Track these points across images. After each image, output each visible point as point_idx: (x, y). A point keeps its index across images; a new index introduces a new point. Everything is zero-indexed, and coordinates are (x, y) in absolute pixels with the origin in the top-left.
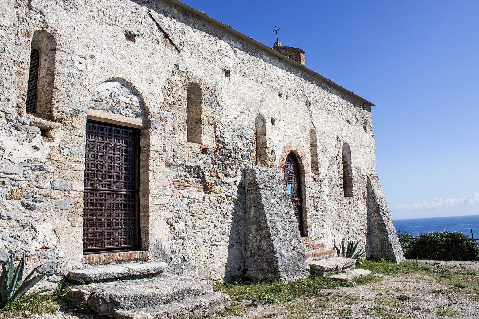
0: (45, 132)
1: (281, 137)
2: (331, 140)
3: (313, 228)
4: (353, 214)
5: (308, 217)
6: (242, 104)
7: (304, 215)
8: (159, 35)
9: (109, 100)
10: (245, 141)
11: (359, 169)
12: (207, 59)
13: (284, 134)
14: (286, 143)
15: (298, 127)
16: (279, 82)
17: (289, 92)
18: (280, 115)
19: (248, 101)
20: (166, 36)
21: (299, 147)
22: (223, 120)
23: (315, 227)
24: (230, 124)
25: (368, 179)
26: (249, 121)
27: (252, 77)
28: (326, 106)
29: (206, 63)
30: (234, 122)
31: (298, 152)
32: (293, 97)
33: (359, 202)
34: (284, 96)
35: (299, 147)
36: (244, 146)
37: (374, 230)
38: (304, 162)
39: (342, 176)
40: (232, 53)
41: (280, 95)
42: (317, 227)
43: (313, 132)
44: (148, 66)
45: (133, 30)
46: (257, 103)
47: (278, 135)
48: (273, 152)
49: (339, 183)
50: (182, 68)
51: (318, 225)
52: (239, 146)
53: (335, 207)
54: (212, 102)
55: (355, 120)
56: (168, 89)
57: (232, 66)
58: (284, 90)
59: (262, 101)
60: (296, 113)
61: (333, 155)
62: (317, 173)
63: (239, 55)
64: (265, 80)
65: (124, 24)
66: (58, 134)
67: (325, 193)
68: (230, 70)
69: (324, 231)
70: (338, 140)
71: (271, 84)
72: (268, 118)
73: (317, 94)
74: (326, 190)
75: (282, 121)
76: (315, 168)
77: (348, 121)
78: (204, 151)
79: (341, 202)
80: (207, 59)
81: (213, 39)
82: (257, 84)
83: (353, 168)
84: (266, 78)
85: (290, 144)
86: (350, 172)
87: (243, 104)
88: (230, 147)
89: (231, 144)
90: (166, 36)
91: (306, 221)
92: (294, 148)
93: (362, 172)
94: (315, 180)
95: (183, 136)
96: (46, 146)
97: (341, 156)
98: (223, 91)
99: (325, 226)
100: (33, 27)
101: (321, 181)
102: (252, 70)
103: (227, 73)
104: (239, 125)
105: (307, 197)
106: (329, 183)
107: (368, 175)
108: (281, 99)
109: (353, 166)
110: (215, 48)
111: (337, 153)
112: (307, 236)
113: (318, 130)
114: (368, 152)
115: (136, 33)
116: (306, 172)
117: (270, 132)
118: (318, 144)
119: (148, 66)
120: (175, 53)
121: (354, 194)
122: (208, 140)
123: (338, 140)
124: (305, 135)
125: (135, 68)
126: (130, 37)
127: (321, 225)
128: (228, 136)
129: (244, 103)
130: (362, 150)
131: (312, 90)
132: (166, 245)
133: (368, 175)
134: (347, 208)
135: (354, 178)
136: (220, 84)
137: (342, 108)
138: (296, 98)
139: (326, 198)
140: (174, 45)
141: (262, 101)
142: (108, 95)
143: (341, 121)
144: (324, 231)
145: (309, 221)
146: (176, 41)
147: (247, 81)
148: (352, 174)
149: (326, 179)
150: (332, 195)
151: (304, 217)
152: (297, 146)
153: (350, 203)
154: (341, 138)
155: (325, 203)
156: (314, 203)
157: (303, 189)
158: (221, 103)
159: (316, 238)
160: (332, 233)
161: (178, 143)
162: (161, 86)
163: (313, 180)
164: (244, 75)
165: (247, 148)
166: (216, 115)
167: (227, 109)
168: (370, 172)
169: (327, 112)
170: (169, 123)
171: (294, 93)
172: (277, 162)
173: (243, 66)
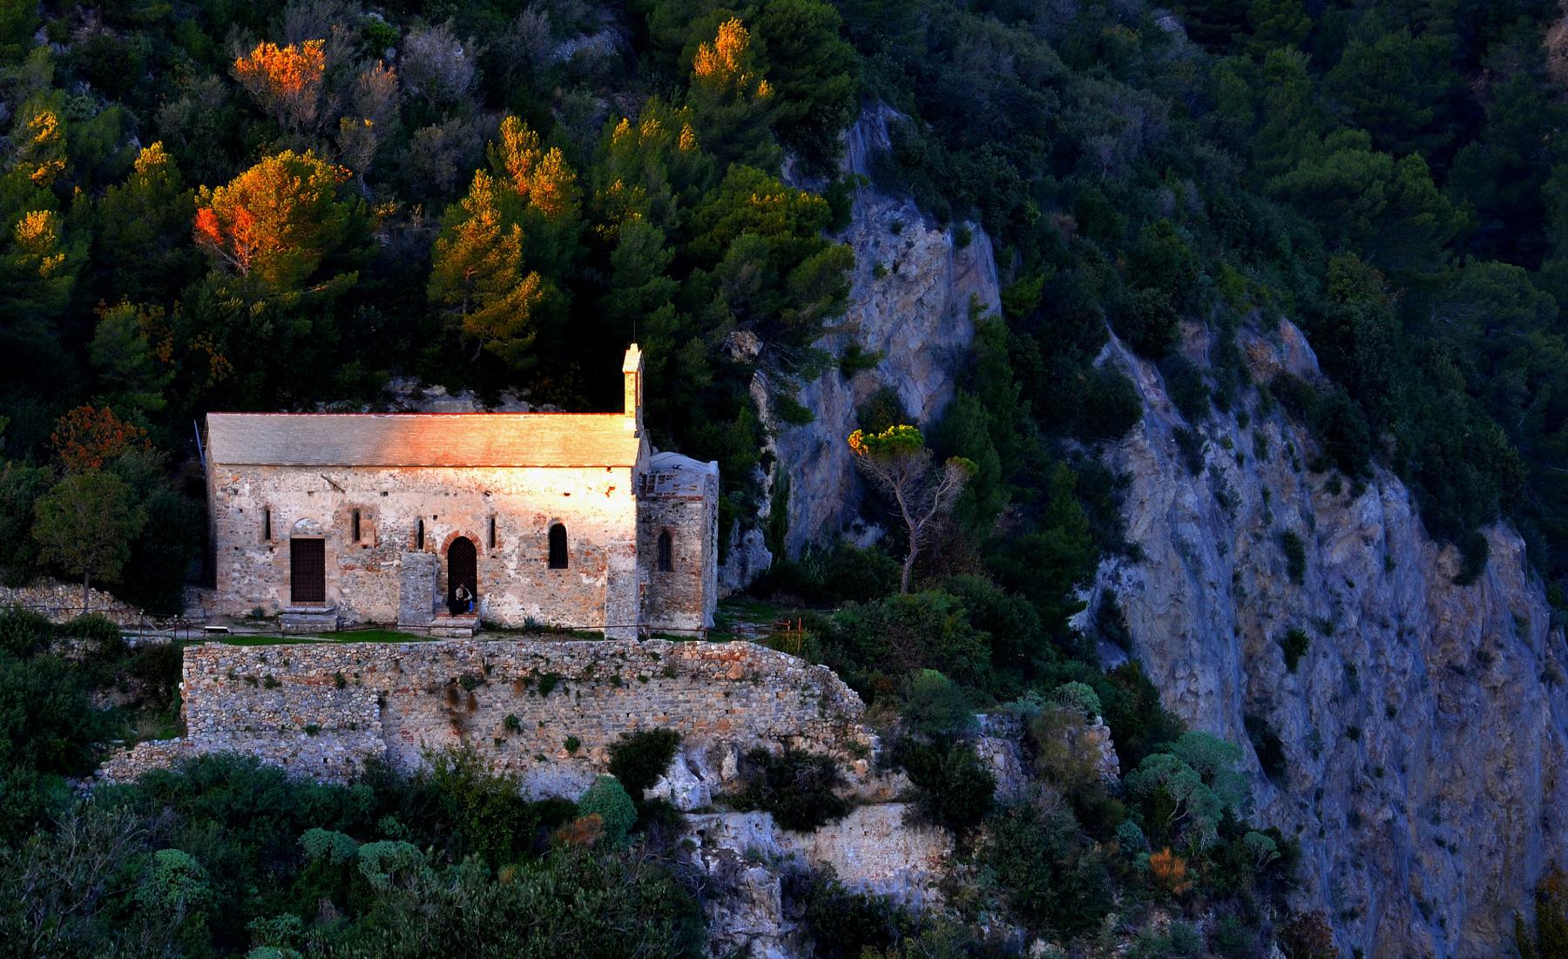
0: (271, 549)
1: (445, 528)
8: (328, 486)
10: (403, 537)
22: (381, 527)
26: (408, 522)
34: (451, 495)
38: (476, 545)
44: (323, 507)
49: (538, 557)
50: (347, 501)
56: (337, 516)
58: (451, 491)
65: (306, 488)
66: (276, 550)
78: (365, 547)
85: (457, 532)
95: (349, 541)
96: (271, 556)
100: (261, 505)
103: (386, 494)
110: (373, 481)
117: (429, 525)
120: (340, 494)
122: (365, 540)
126: (310, 493)
132: (337, 600)
139: (512, 573)
144: (505, 599)
146: (342, 487)
147: (405, 494)
164: (403, 491)
172: (439, 547)
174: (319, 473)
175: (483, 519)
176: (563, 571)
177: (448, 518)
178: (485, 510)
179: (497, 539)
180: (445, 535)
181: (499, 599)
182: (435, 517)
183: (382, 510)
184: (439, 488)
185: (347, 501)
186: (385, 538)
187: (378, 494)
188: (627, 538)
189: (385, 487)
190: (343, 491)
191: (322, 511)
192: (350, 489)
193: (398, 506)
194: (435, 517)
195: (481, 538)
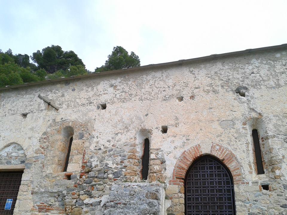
1: (178, 142)
6: (118, 126)
9: (6, 157)
10: (119, 159)
12: (83, 105)
13: (184, 139)
14: (187, 148)
16: (178, 87)
19: (126, 121)
20: (49, 104)
21: (218, 147)
24: (102, 147)
27: (133, 99)
29: (81, 108)
30: (107, 144)
31: (215, 154)
36: (117, 164)
38: (231, 166)
40: (111, 90)
41: (181, 99)
45: (24, 112)
46: (140, 119)
47: (173, 142)
50: (58, 119)
52: (110, 164)
54: (83, 135)
57: (109, 99)
59: (147, 115)
63: (118, 88)
64: (153, 94)
68: (107, 103)
71: (164, 93)
72: (157, 128)
80: (83, 105)
81: (90, 89)
82: (141, 101)
84: (156, 90)
85: (198, 147)
87: (120, 126)
88: (99, 168)
89: (99, 166)
90: (49, 104)
92: (205, 150)
98: (96, 122)
102: (134, 93)
103: (104, 107)
104: (113, 146)
115: (28, 112)
119: (32, 129)
125: (22, 133)
128: (96, 159)
129: (121, 124)
136: (93, 118)
140: (54, 108)
141: (147, 115)
142: (6, 154)
147: (126, 105)
158: (94, 133)
161: (44, 174)
162: (38, 138)
164: (123, 100)
165: (121, 165)
166: (87, 144)
167: (99, 136)
170: (40, 162)
173: (123, 94)
174: (37, 94)
175: (239, 125)
177: (183, 129)
179: (266, 158)
180: (178, 153)
182: (165, 130)
183: (98, 126)
184: (169, 92)
185: (58, 119)
186: (95, 162)
187: (93, 107)
189: (102, 99)
190: (57, 109)
191: (30, 134)
192: (64, 106)
193: (117, 118)
194: (165, 130)
195: (238, 155)
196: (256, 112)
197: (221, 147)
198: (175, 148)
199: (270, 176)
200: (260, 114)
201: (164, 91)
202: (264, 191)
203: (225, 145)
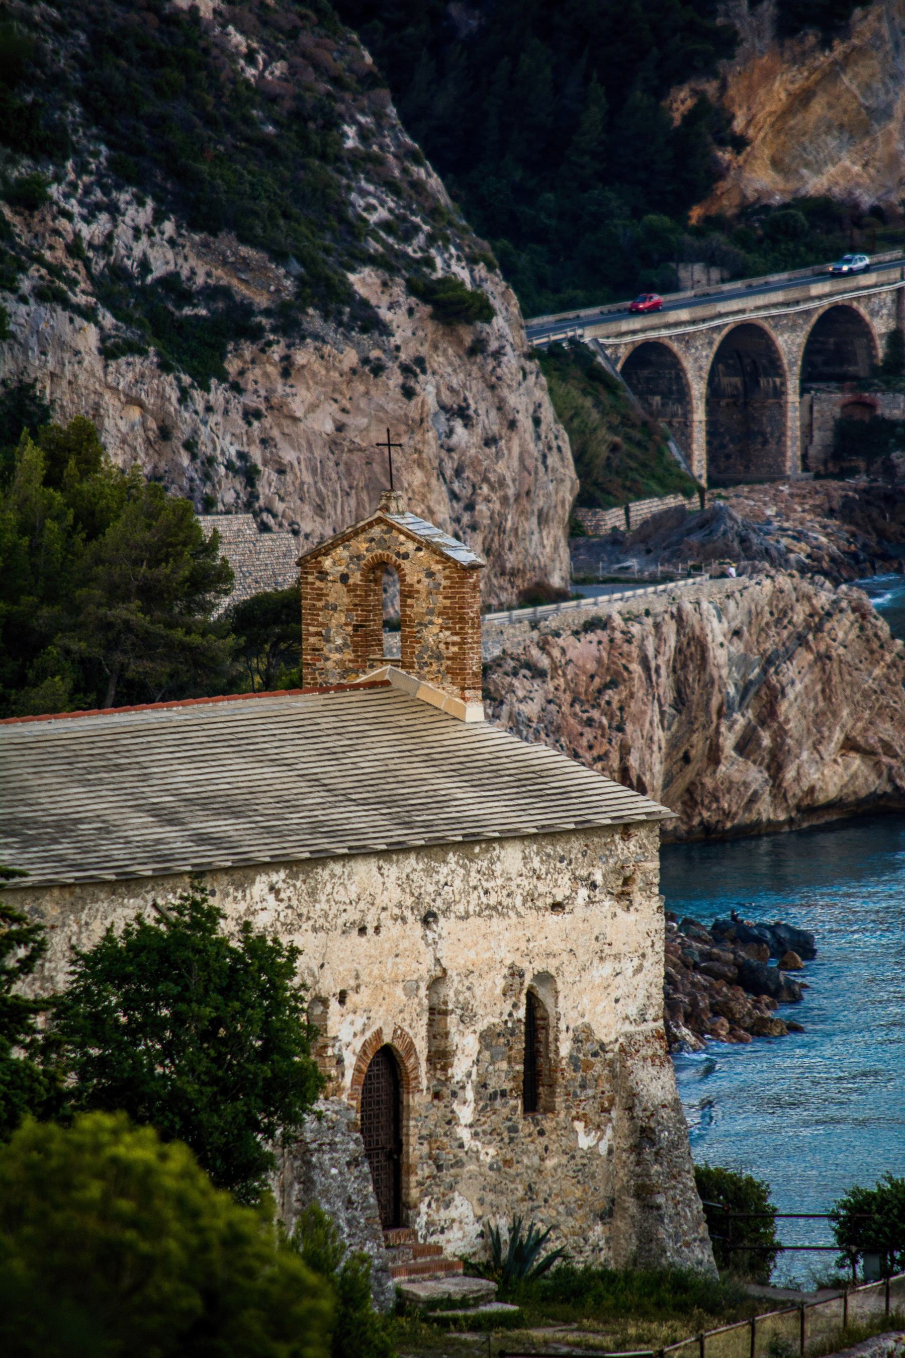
2: (490, 984)
3: (423, 1208)
4: (550, 1163)
5: (413, 1184)
7: (404, 1178)
11: (582, 1036)
14: (368, 1035)
15: (399, 991)
17: (384, 915)
18: (357, 977)
21: (399, 1032)
23: (429, 1206)
25: (622, 1050)
28: (484, 899)
32: (390, 923)
33: (579, 1126)
34: (370, 931)
35: (399, 1032)
37: (625, 1201)
39: (520, 1068)
41: (362, 931)
42: (434, 1205)
43: (437, 982)
47: (352, 1023)
48: (340, 1061)
49: (507, 1086)
51: (437, 1200)
53: (489, 1153)
55: (583, 893)
60: (397, 956)
61: (496, 1021)
62: (443, 1078)
67: (463, 1122)
69: (453, 1213)
70: (516, 973)
73: (458, 883)
74: (466, 1113)
75: (363, 988)
76: (439, 1066)
77: (557, 907)
79: (513, 1135)
83: (562, 1036)
85: (379, 1033)
86: (552, 1047)
91: (408, 1195)
92: (387, 1039)
93: (602, 1034)
94: (437, 1096)
97: (521, 1013)
99: (458, 1199)
101: (454, 1094)
105: (413, 1140)
106: (477, 1093)
107: (621, 1040)
108: (364, 940)
109: (562, 1026)
111: (508, 1008)
112: (408, 1227)
113: (454, 974)
114: (630, 972)
116: (413, 1084)
118: (451, 1007)
121: (559, 1102)
123: (516, 973)
124: (416, 1000)
127: (447, 1198)
130: (607, 968)
131: (442, 882)
133: (621, 1040)
134: (531, 1147)
135: (564, 1062)
137: (539, 878)
138: (399, 921)
139: (464, 1134)
143: (531, 917)
144: (453, 1213)
145: (414, 1193)
148: (557, 1051)
149: (469, 1087)
150: (485, 1123)
151: (404, 1185)
152: (395, 1032)
153: (541, 1133)
154: (524, 965)
155: (461, 1146)
156: (431, 1149)
157: (405, 1123)
159: (432, 1230)
160: (475, 1216)
163: (429, 1098)
168: (631, 1028)
169: (487, 912)
171: (396, 911)
172: (347, 1081)
176: (548, 1125)
178: (425, 968)
180: (358, 1044)
181: (444, 1214)
182: (342, 998)
188: (651, 1013)
196: (441, 965)
197: (402, 1030)
198: (355, 1035)
199: (438, 1076)
200: (444, 971)
201: (345, 911)
202: (436, 1102)
203: (407, 1029)
